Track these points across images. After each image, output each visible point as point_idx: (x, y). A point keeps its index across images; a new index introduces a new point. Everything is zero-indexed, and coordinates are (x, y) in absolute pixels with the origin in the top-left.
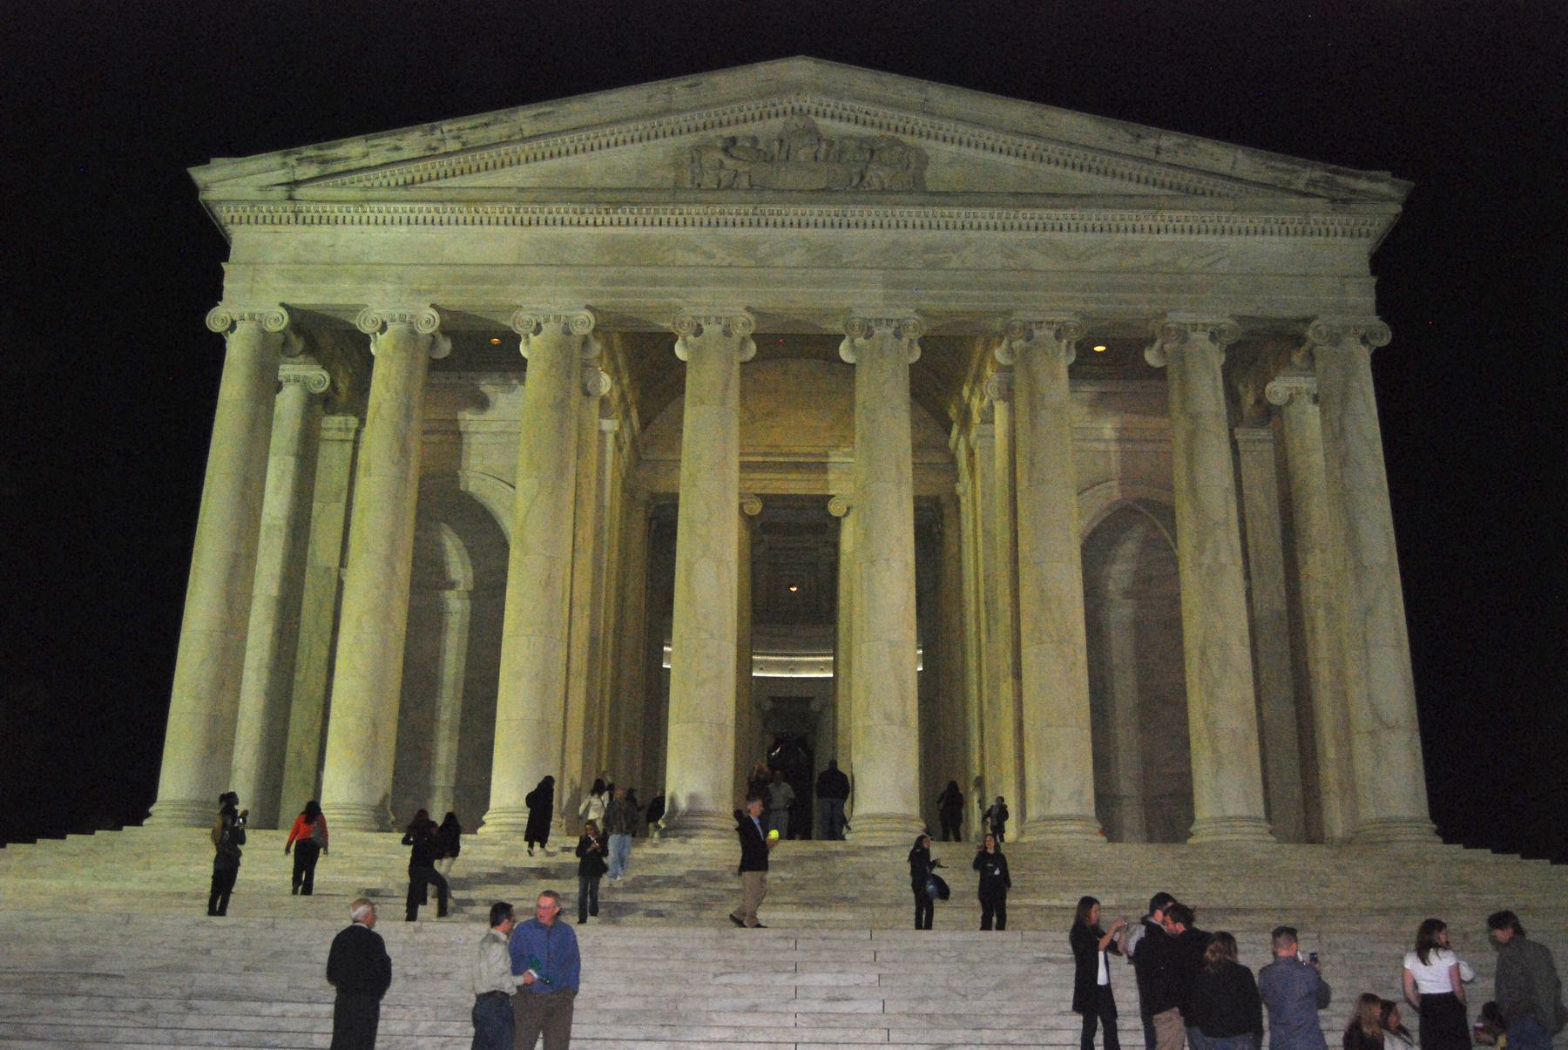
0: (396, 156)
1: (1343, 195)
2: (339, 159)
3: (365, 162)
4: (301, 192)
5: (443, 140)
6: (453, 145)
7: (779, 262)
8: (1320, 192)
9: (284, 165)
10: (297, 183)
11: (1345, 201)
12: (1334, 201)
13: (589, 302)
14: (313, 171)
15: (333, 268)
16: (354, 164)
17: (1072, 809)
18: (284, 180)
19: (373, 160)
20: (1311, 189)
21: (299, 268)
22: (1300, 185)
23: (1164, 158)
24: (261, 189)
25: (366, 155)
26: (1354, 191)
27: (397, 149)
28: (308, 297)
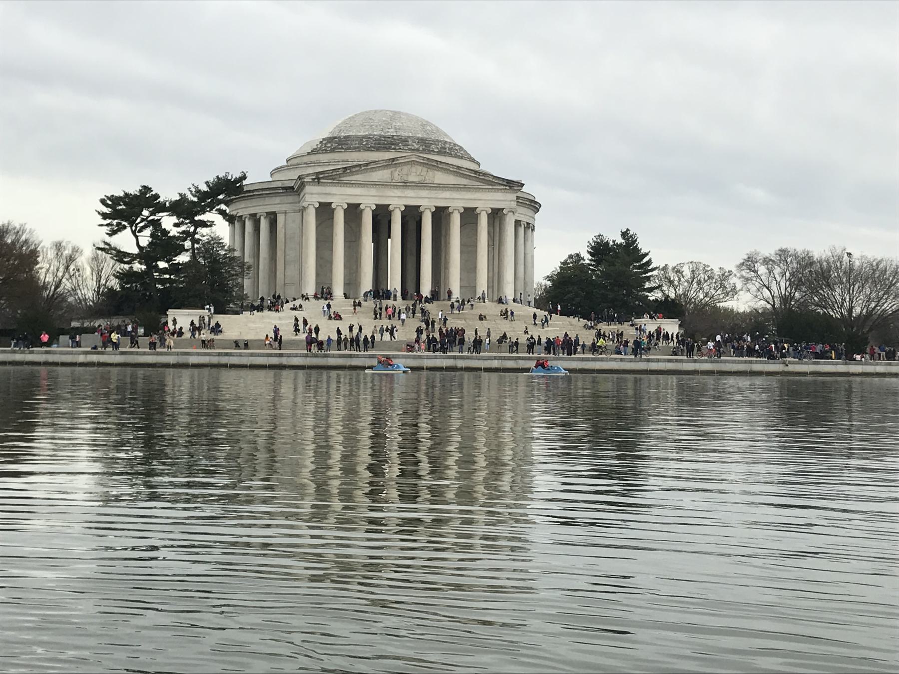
14: (321, 176)
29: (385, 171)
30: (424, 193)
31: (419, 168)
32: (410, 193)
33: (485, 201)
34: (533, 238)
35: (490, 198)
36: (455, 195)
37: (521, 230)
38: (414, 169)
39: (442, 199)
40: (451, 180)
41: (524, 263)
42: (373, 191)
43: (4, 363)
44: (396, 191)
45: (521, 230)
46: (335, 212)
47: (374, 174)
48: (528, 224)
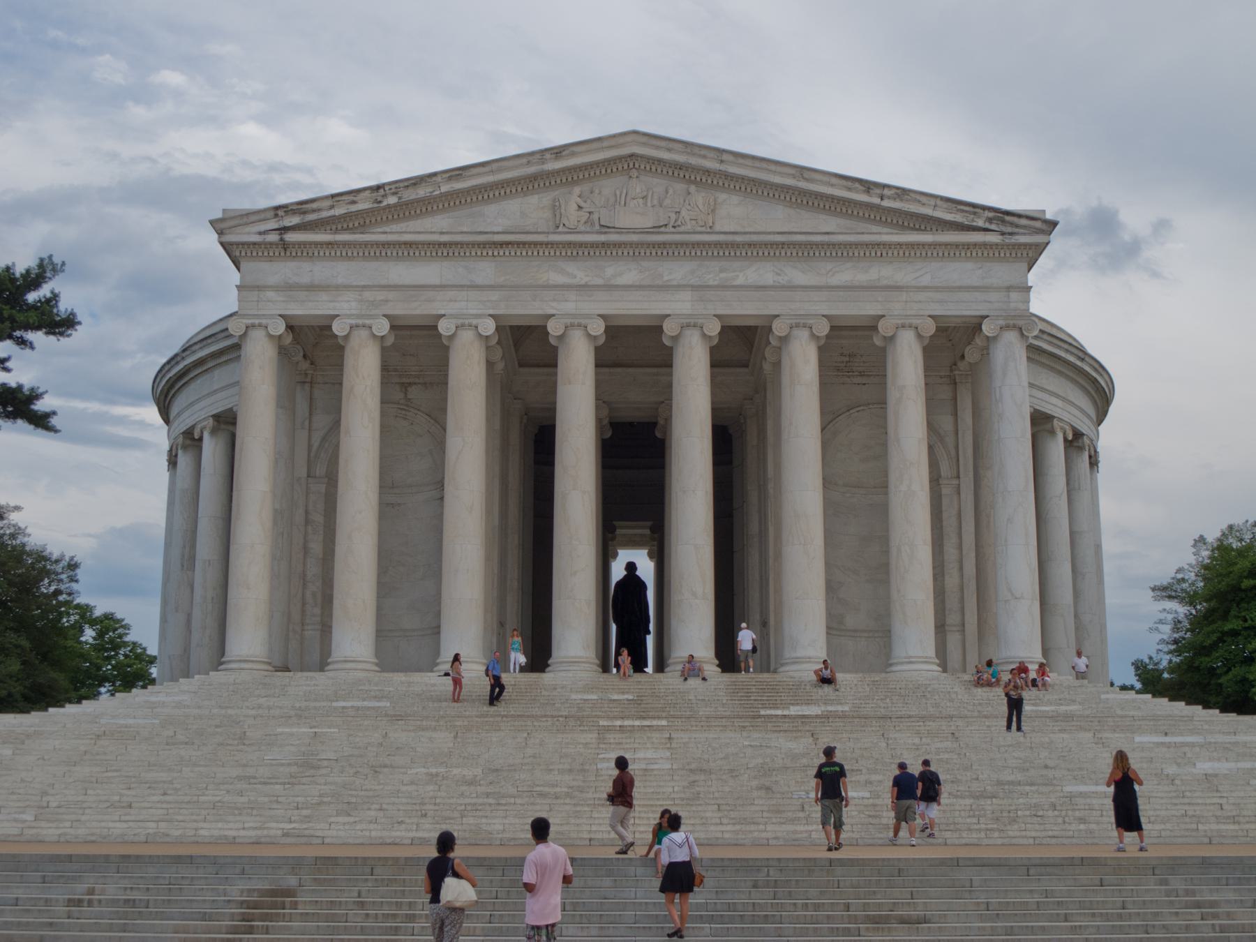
0: (354, 208)
1: (1009, 229)
2: (314, 211)
3: (332, 213)
4: (291, 237)
5: (385, 196)
6: (392, 200)
7: (620, 281)
8: (993, 227)
9: (276, 215)
10: (284, 230)
11: (1011, 234)
12: (1003, 234)
13: (491, 312)
15: (312, 288)
16: (325, 214)
17: (810, 652)
18: (276, 226)
19: (338, 211)
20: (987, 225)
21: (288, 288)
22: (980, 223)
23: (886, 203)
24: (260, 233)
25: (332, 207)
26: (1017, 226)
27: (354, 202)
28: (296, 310)
29: (534, 200)
30: (676, 271)
31: (658, 184)
32: (628, 273)
33: (912, 296)
34: (1093, 481)
35: (926, 280)
36: (796, 274)
37: (1056, 450)
38: (637, 187)
39: (749, 291)
40: (776, 220)
41: (1067, 552)
42: (485, 270)
43: (7, 925)
44: (571, 267)
45: (1056, 450)
46: (348, 354)
47: (491, 210)
48: (1078, 435)
